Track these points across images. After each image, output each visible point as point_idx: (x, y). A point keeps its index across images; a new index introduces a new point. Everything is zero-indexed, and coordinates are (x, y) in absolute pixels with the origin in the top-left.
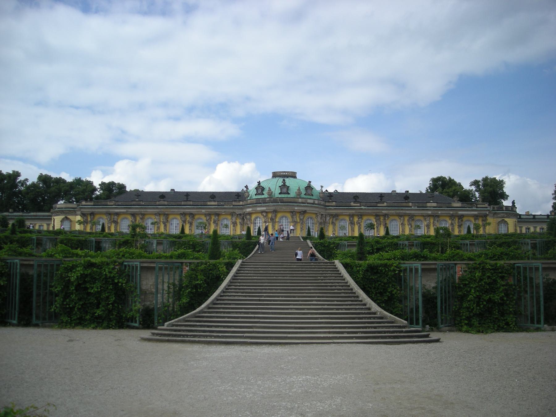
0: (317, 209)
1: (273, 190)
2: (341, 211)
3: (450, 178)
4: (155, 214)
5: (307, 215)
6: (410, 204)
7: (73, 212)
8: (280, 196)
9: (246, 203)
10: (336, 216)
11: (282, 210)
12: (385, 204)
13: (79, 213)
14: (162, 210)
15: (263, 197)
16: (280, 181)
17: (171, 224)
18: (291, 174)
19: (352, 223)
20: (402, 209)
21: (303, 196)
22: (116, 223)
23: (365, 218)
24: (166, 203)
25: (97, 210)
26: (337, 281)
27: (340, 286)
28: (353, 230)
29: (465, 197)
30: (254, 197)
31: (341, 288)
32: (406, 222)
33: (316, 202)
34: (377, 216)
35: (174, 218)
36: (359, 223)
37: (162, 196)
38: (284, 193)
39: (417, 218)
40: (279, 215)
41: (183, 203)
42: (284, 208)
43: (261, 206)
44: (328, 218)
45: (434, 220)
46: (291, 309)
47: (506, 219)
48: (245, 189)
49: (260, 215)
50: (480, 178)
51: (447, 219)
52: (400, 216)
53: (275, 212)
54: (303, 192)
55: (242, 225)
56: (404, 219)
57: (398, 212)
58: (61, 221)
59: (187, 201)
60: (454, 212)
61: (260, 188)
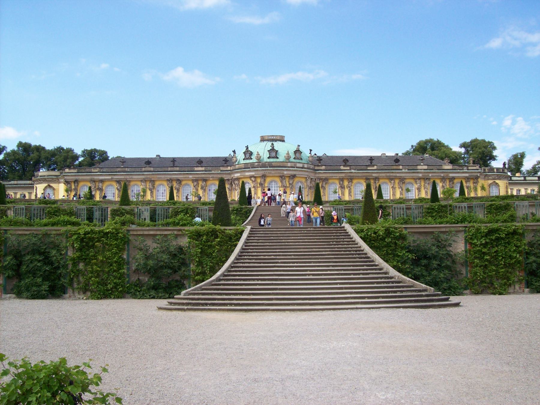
0: (307, 174)
1: (261, 154)
2: (331, 175)
3: (438, 140)
4: (141, 181)
5: (296, 180)
6: (401, 167)
7: (56, 180)
8: (269, 160)
9: (234, 168)
11: (271, 175)
12: (375, 167)
13: (62, 180)
14: (148, 176)
15: (251, 161)
16: (268, 146)
17: (158, 191)
18: (279, 138)
19: (342, 187)
20: (392, 172)
21: (292, 160)
23: (355, 181)
24: (152, 169)
25: (80, 178)
26: (350, 246)
27: (353, 251)
28: (343, 194)
29: (454, 159)
30: (242, 162)
31: (355, 252)
32: (397, 185)
33: (306, 166)
35: (160, 185)
37: (148, 162)
38: (273, 158)
39: (407, 181)
40: (268, 180)
41: (169, 169)
42: (273, 172)
43: (250, 171)
45: (425, 183)
46: (309, 275)
47: (497, 181)
48: (232, 154)
49: (249, 180)
50: (468, 140)
52: (391, 179)
53: (264, 177)
54: (292, 156)
55: (230, 190)
56: (394, 182)
57: (388, 175)
58: (44, 190)
59: (173, 166)
60: (445, 174)
61: (248, 154)
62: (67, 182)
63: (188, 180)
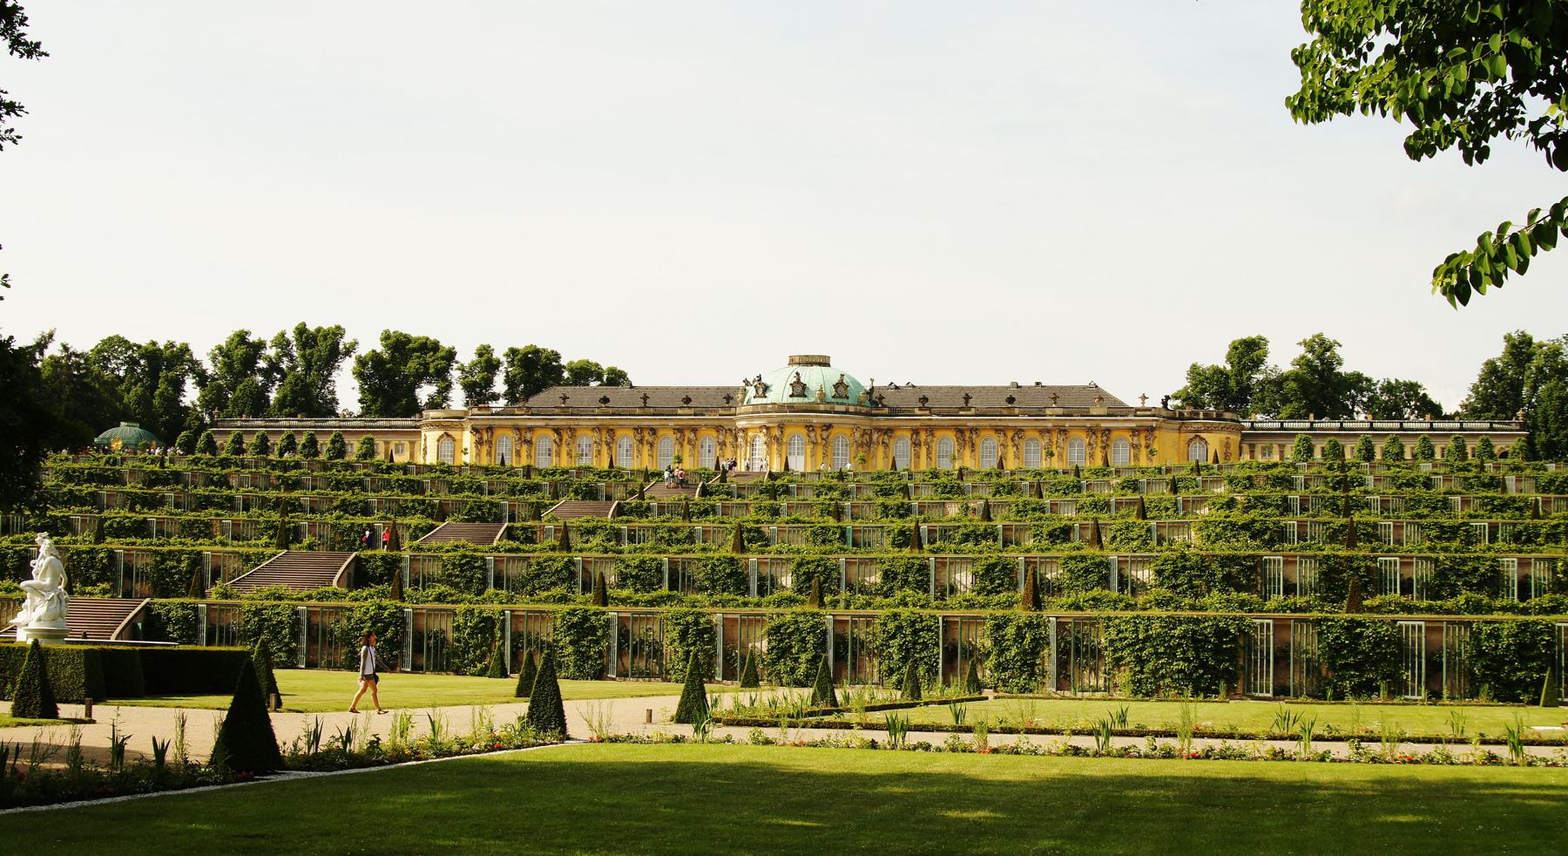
5: (834, 431)
8: (791, 400)
10: (889, 431)
12: (973, 411)
15: (764, 401)
19: (917, 444)
22: (529, 442)
23: (938, 434)
28: (918, 456)
32: (1010, 443)
34: (960, 431)
36: (927, 443)
40: (788, 431)
44: (875, 436)
47: (1203, 435)
51: (1083, 435)
52: (998, 430)
53: (781, 427)
54: (830, 392)
62: (475, 430)
63: (665, 427)
